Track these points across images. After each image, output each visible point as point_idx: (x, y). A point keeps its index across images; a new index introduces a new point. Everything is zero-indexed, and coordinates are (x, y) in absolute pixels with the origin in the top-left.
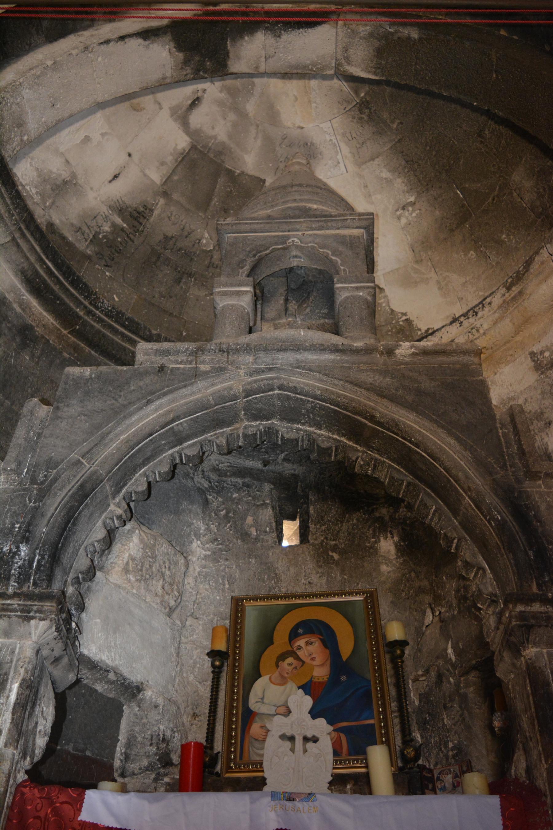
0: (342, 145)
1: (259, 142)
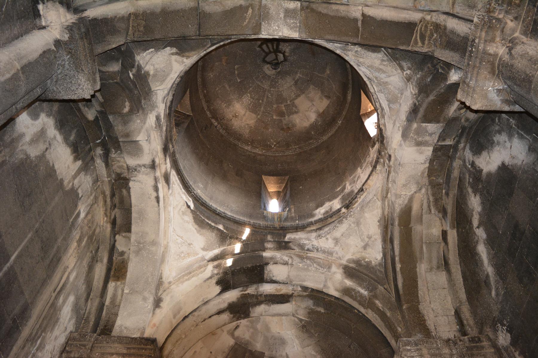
0: (296, 340)
1: (262, 339)
